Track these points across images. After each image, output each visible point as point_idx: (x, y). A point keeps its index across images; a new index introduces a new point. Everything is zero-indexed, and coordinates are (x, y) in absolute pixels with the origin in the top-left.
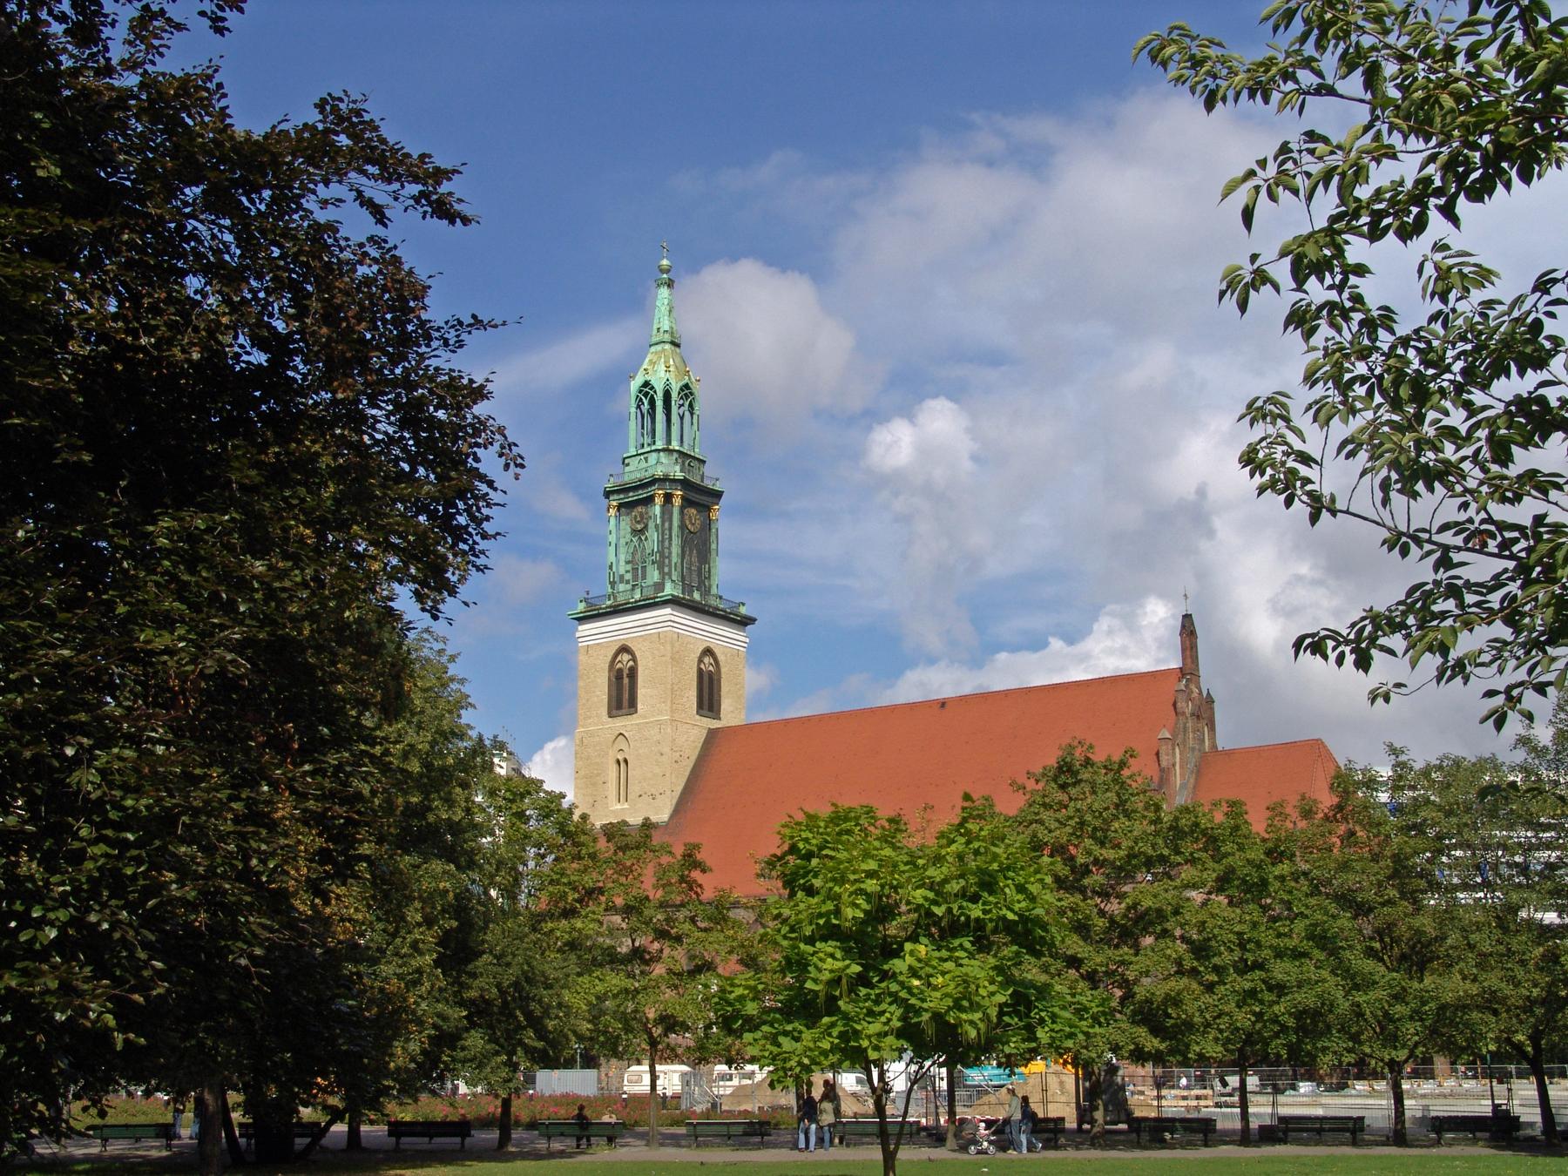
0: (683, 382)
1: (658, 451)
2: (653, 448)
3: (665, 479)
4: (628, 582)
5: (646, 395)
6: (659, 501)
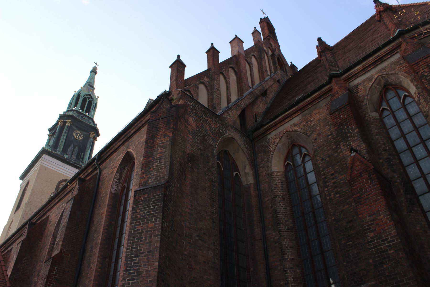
0: (89, 93)
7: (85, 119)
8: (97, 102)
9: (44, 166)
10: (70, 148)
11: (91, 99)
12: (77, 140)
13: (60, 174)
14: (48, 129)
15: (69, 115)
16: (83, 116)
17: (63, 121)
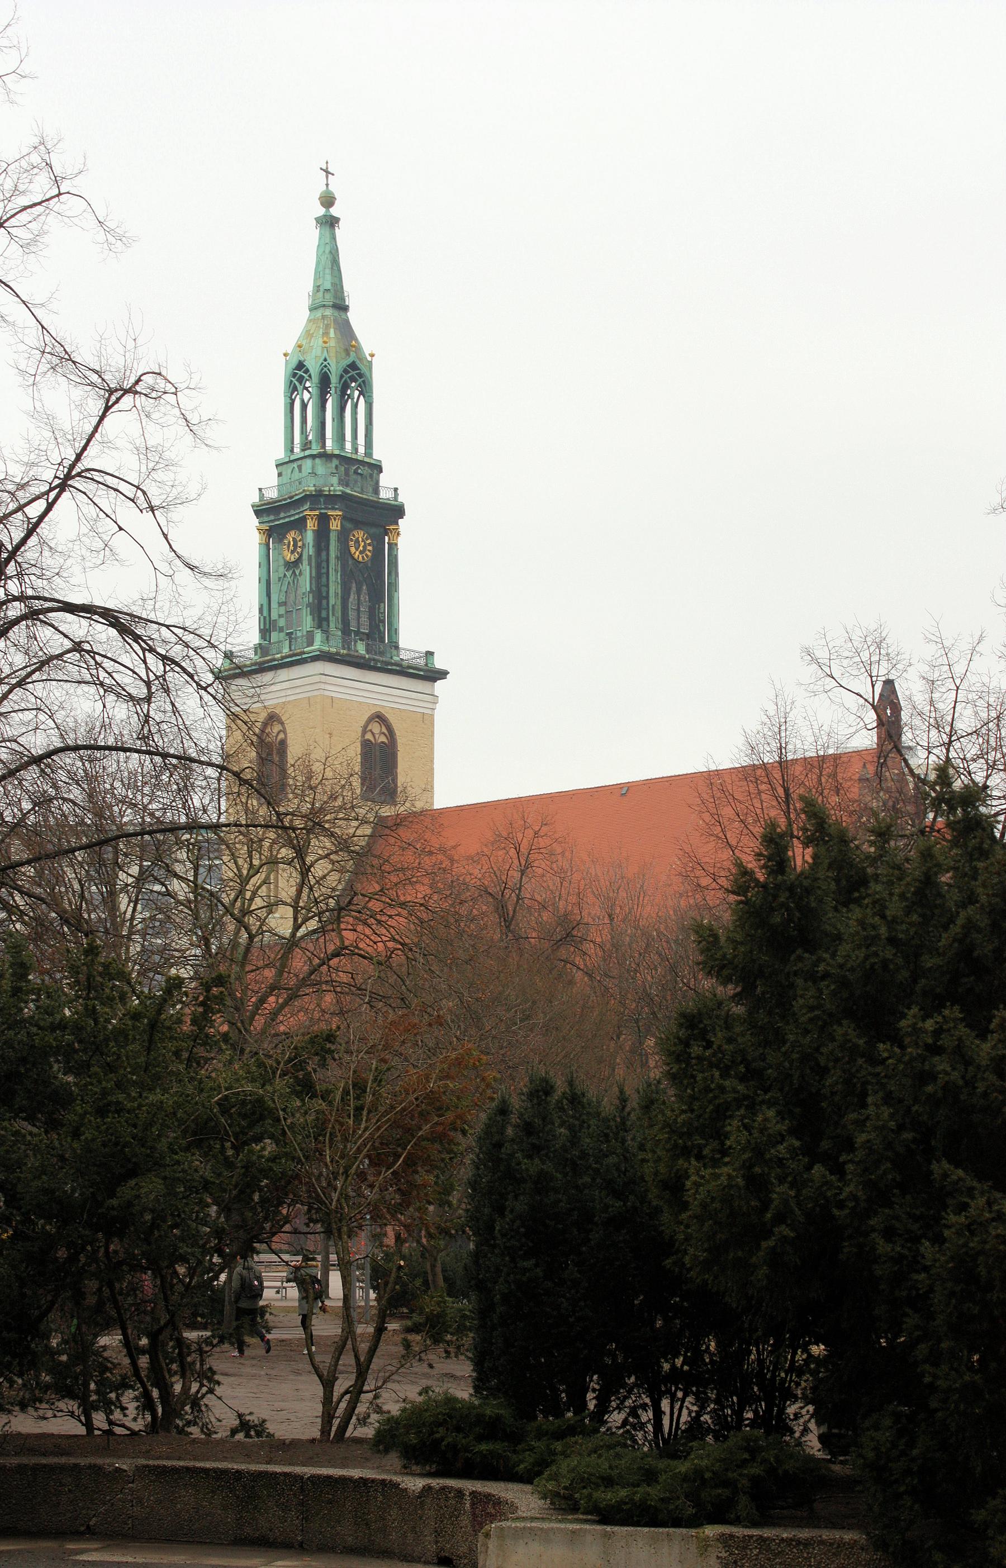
0: (349, 361)
1: (313, 457)
2: (307, 453)
3: (315, 498)
4: (281, 630)
9: (328, 697)
10: (352, 597)
11: (360, 380)
13: (360, 703)
17: (317, 513)
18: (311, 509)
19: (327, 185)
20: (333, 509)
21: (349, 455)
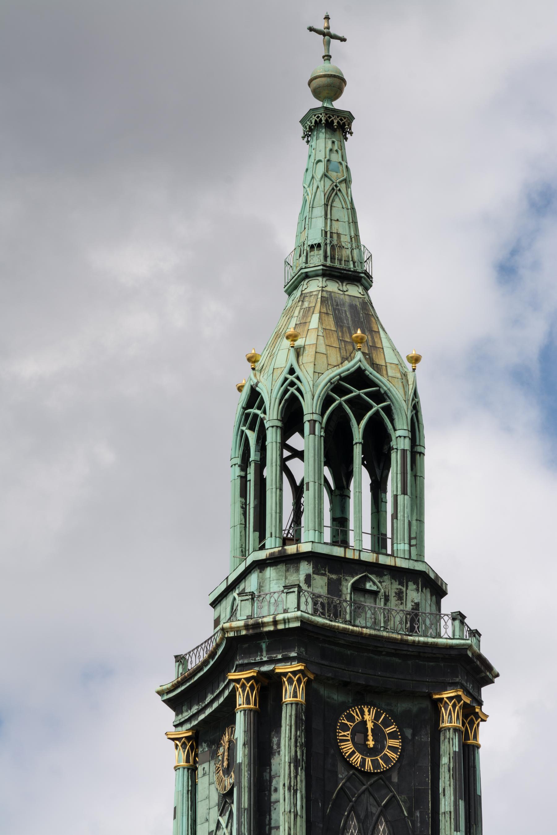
5: (252, 428)
6: (240, 700)
7: (374, 594)
8: (416, 408)
11: (376, 407)
12: (368, 775)
14: (160, 693)
15: (281, 627)
16: (365, 579)
18: (242, 668)
19: (327, 57)
20: (286, 659)
21: (338, 551)
